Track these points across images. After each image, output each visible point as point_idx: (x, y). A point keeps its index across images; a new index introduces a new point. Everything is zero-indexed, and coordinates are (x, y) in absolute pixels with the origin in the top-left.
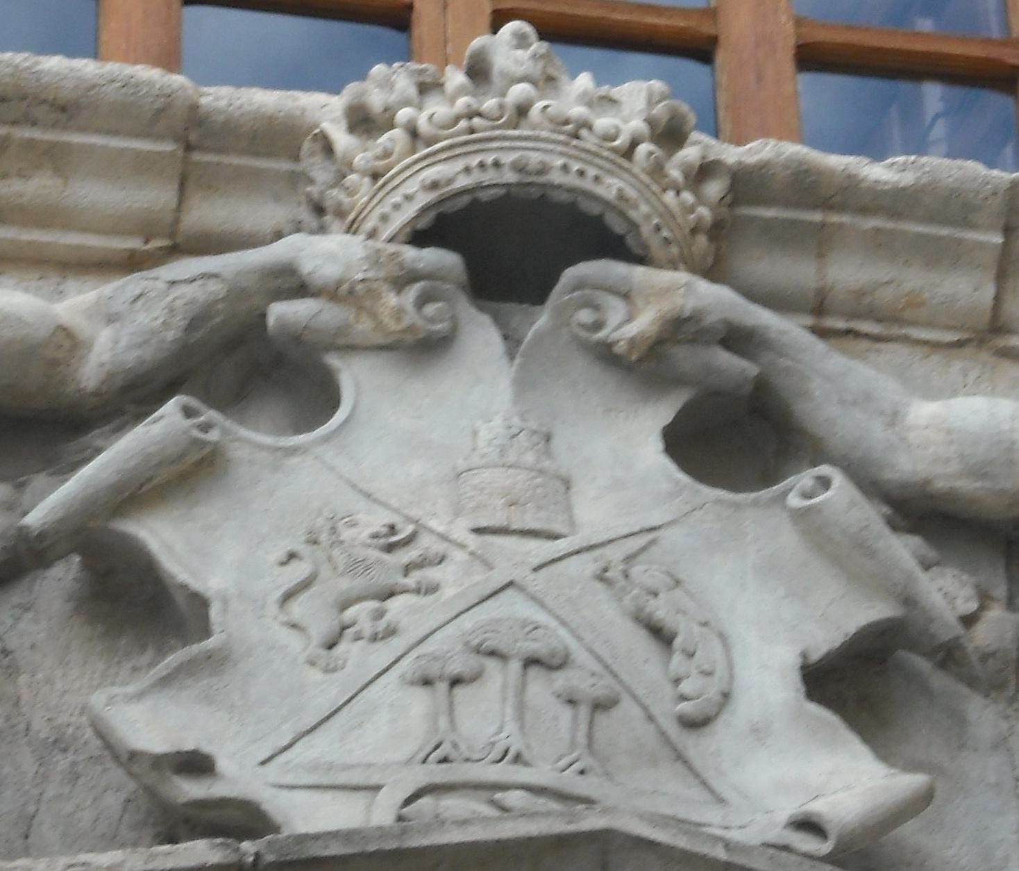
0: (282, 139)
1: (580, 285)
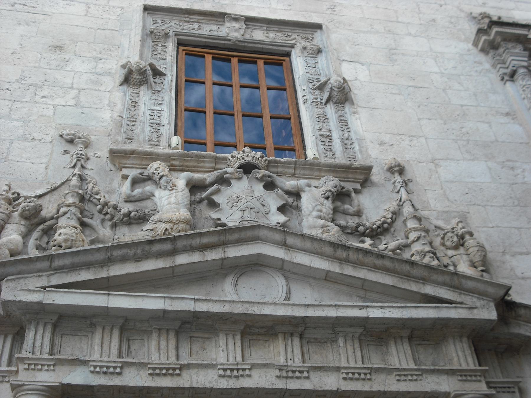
0: (225, 159)
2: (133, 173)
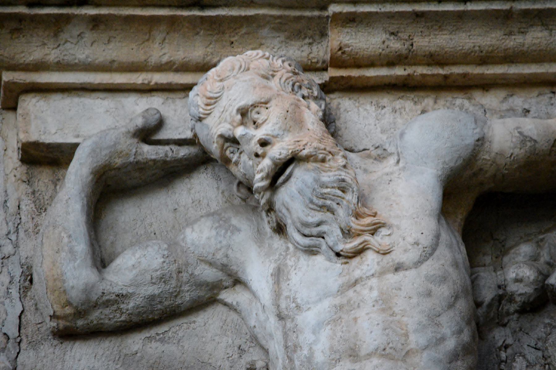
2: (95, 126)
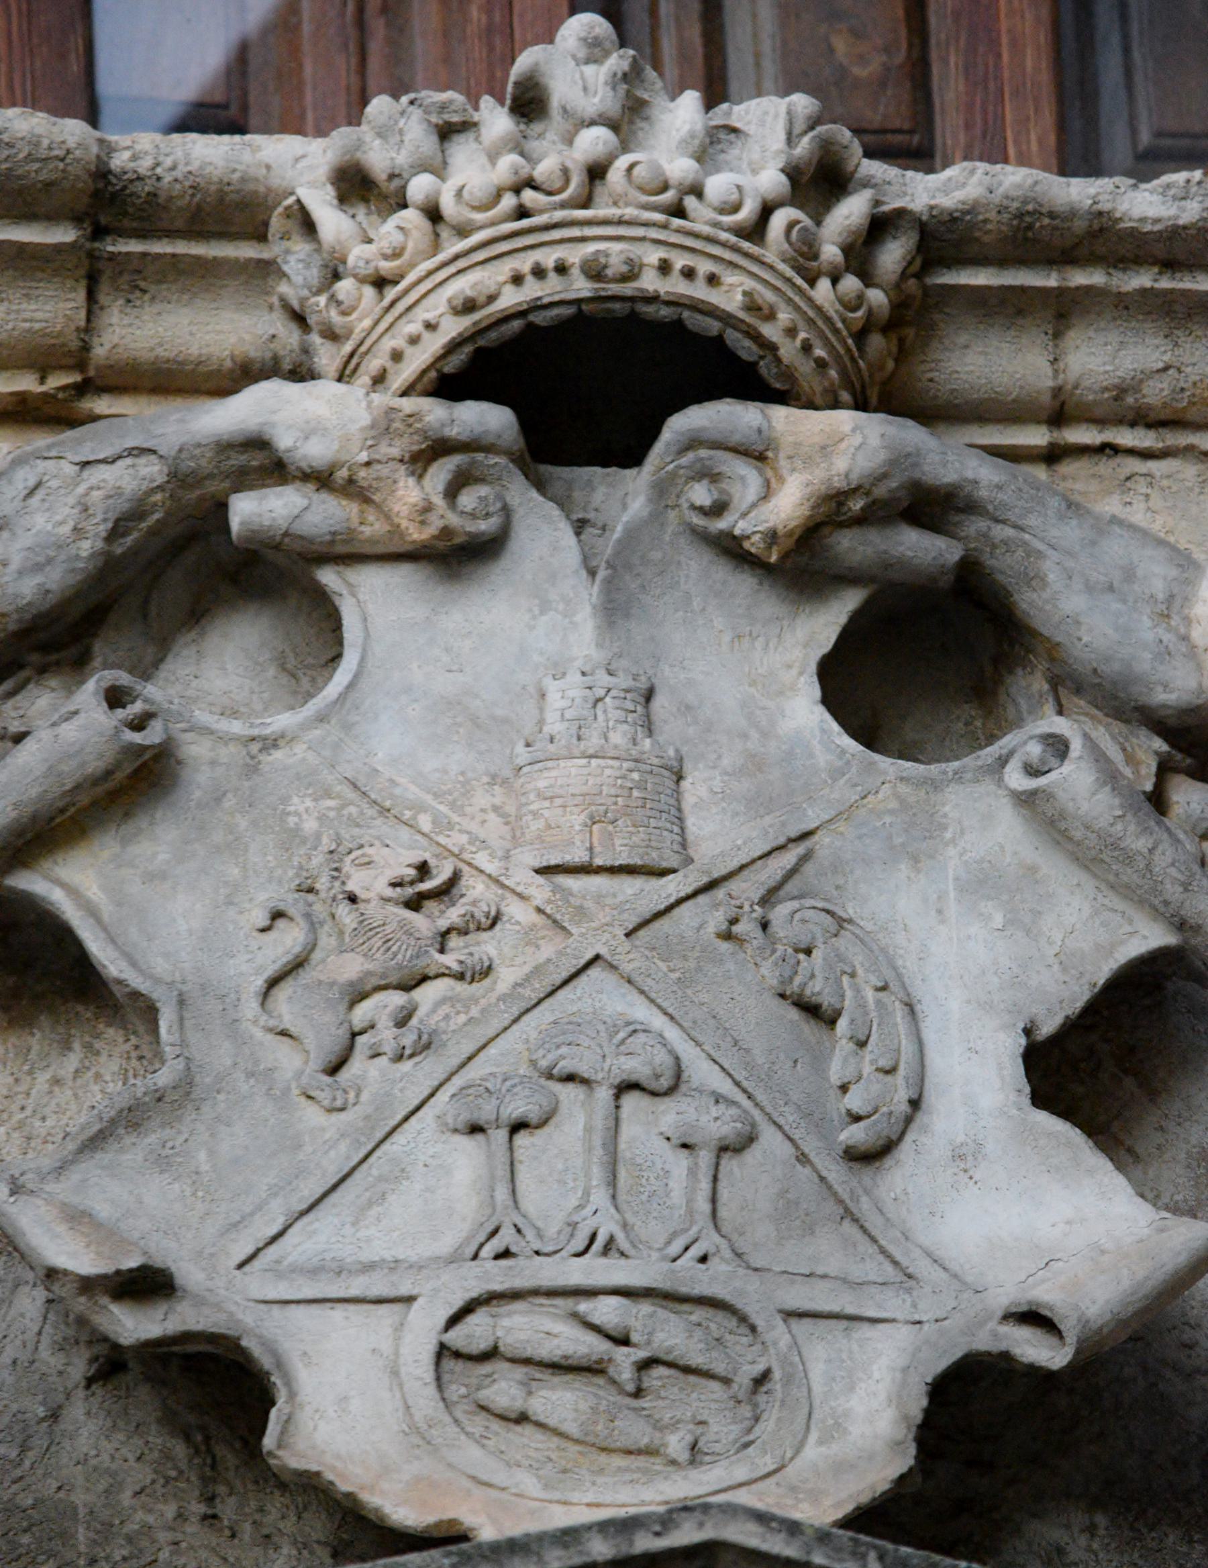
1: (693, 443)
